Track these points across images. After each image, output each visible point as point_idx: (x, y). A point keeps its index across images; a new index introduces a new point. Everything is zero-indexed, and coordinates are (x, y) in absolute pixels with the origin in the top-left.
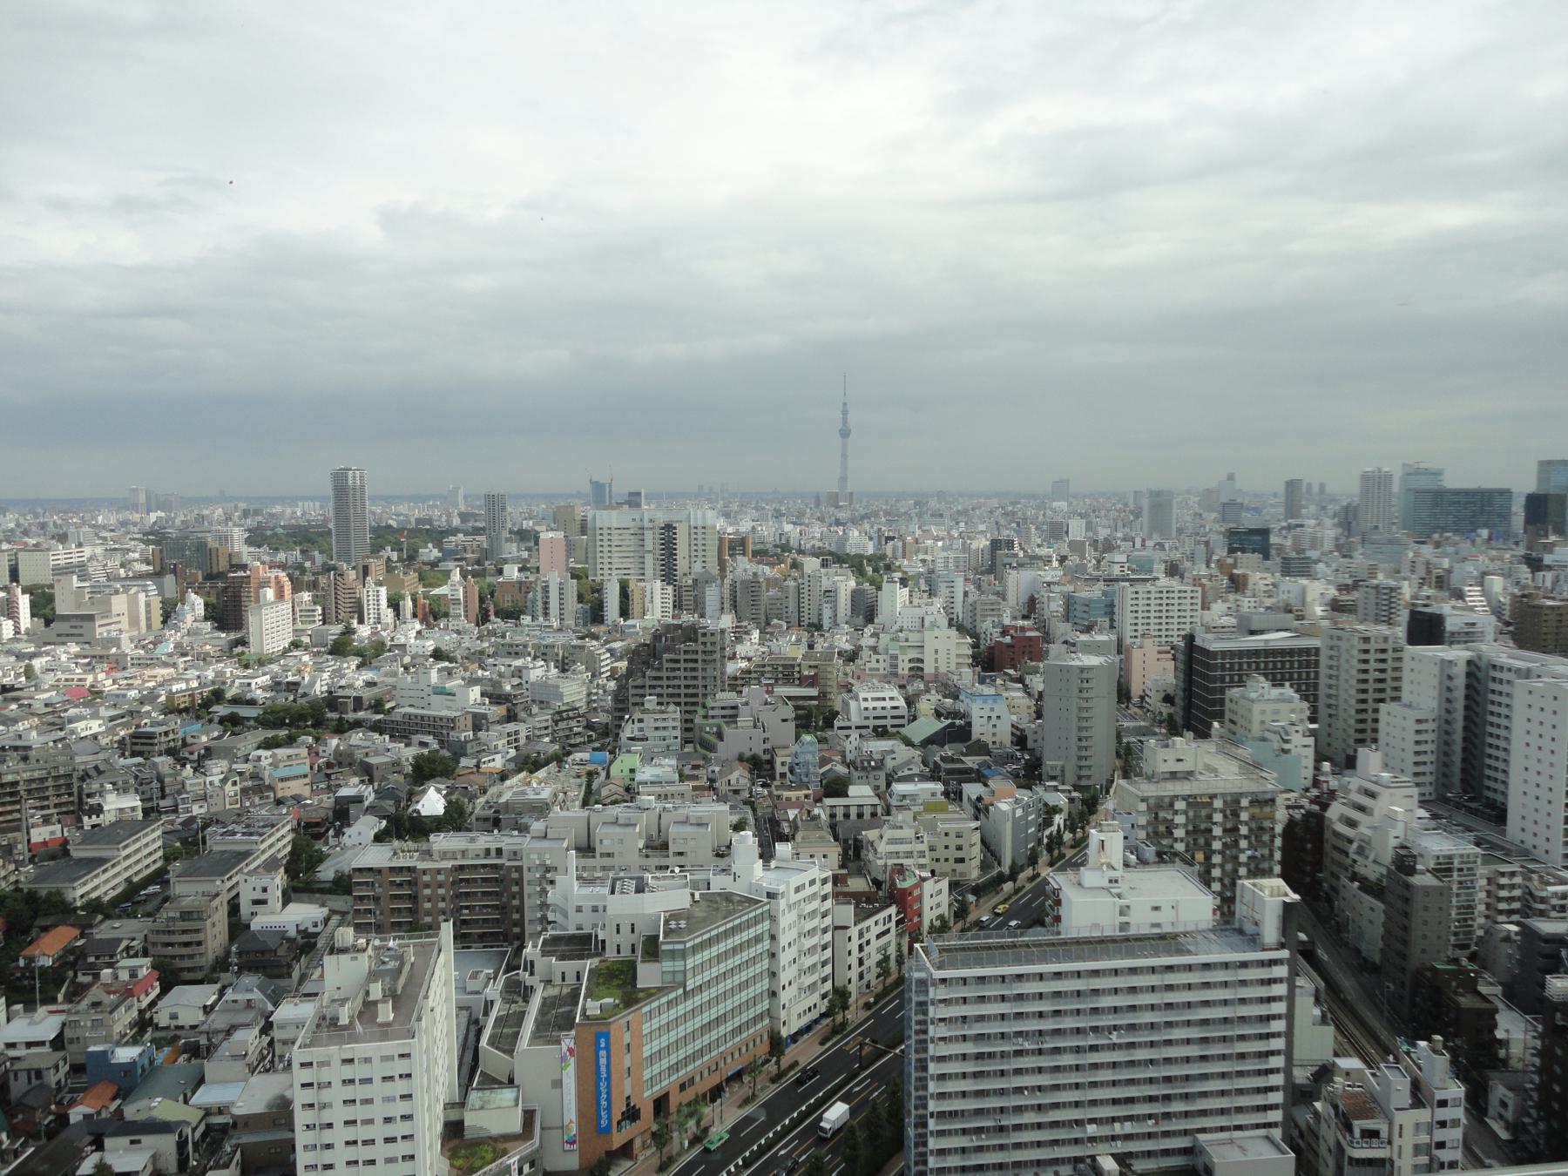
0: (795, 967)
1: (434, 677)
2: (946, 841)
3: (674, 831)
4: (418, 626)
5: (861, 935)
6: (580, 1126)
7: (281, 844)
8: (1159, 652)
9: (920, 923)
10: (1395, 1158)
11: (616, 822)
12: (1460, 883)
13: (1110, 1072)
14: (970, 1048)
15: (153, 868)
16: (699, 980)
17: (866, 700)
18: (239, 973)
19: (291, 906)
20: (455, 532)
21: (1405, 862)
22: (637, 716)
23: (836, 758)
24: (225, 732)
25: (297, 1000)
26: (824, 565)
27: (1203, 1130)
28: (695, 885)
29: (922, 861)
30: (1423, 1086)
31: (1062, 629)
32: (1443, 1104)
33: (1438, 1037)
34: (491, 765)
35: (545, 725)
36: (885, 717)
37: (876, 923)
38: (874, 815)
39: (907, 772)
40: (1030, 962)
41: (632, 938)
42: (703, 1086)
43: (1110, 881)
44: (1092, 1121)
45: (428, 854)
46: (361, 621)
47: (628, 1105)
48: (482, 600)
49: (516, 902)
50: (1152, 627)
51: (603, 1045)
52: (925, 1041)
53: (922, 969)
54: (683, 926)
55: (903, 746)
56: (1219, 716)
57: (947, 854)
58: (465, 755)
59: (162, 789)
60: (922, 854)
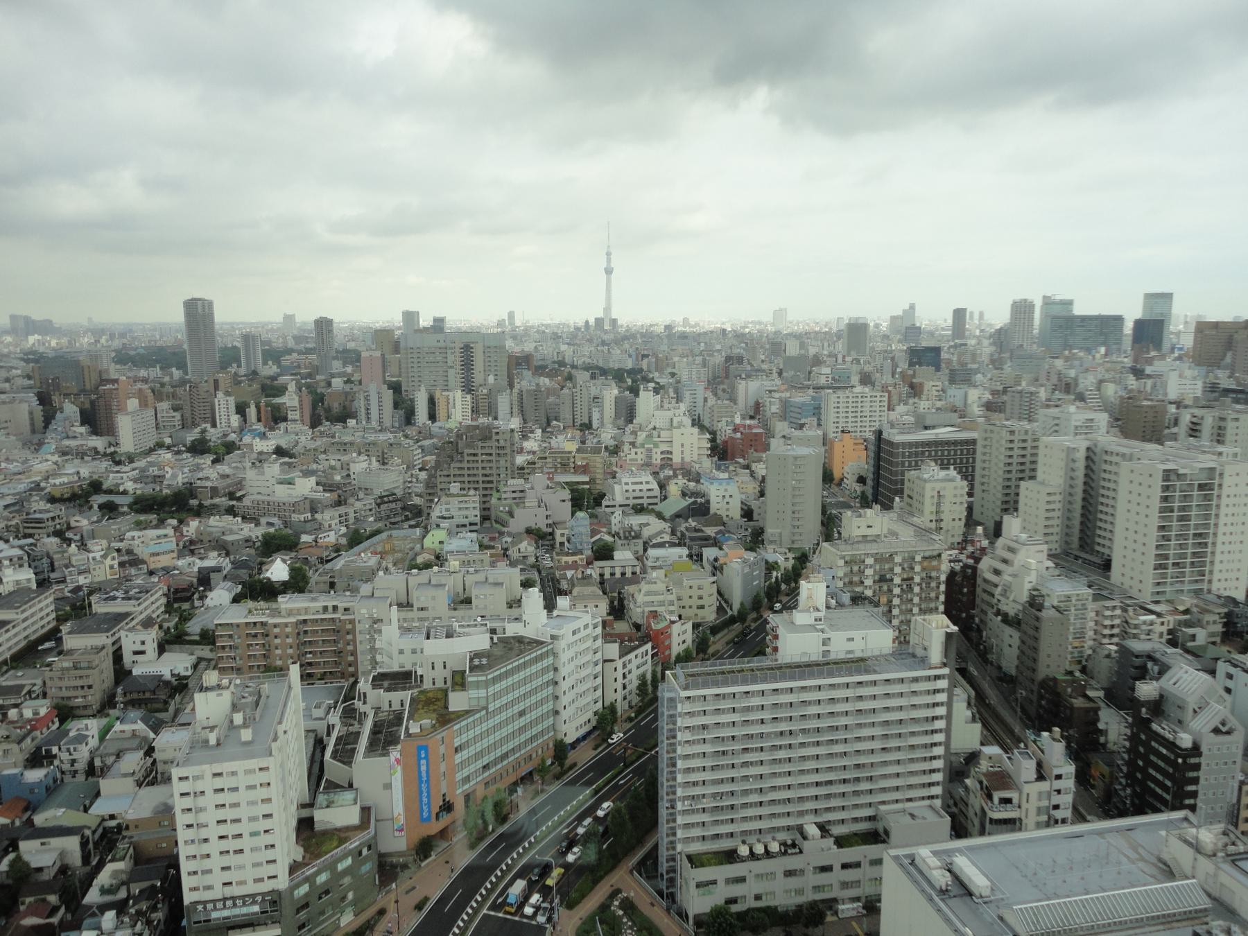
5: (624, 666)
6: (406, 819)
7: (154, 606)
8: (855, 444)
10: (1023, 818)
12: (1076, 615)
13: (813, 762)
14: (708, 748)
15: (51, 626)
16: (498, 704)
17: (627, 484)
18: (125, 708)
19: (165, 654)
20: (289, 351)
21: (1035, 603)
22: (444, 499)
24: (103, 516)
25: (173, 729)
26: (593, 377)
27: (883, 803)
29: (672, 608)
30: (1045, 765)
31: (781, 427)
32: (1059, 777)
33: (1057, 729)
34: (326, 540)
36: (642, 498)
37: (636, 657)
38: (634, 573)
39: (659, 540)
46: (214, 425)
47: (444, 800)
48: (314, 407)
49: (350, 648)
50: (850, 425)
51: (423, 756)
52: (674, 744)
53: (673, 690)
56: (900, 492)
57: (690, 602)
59: (52, 564)
60: (671, 603)
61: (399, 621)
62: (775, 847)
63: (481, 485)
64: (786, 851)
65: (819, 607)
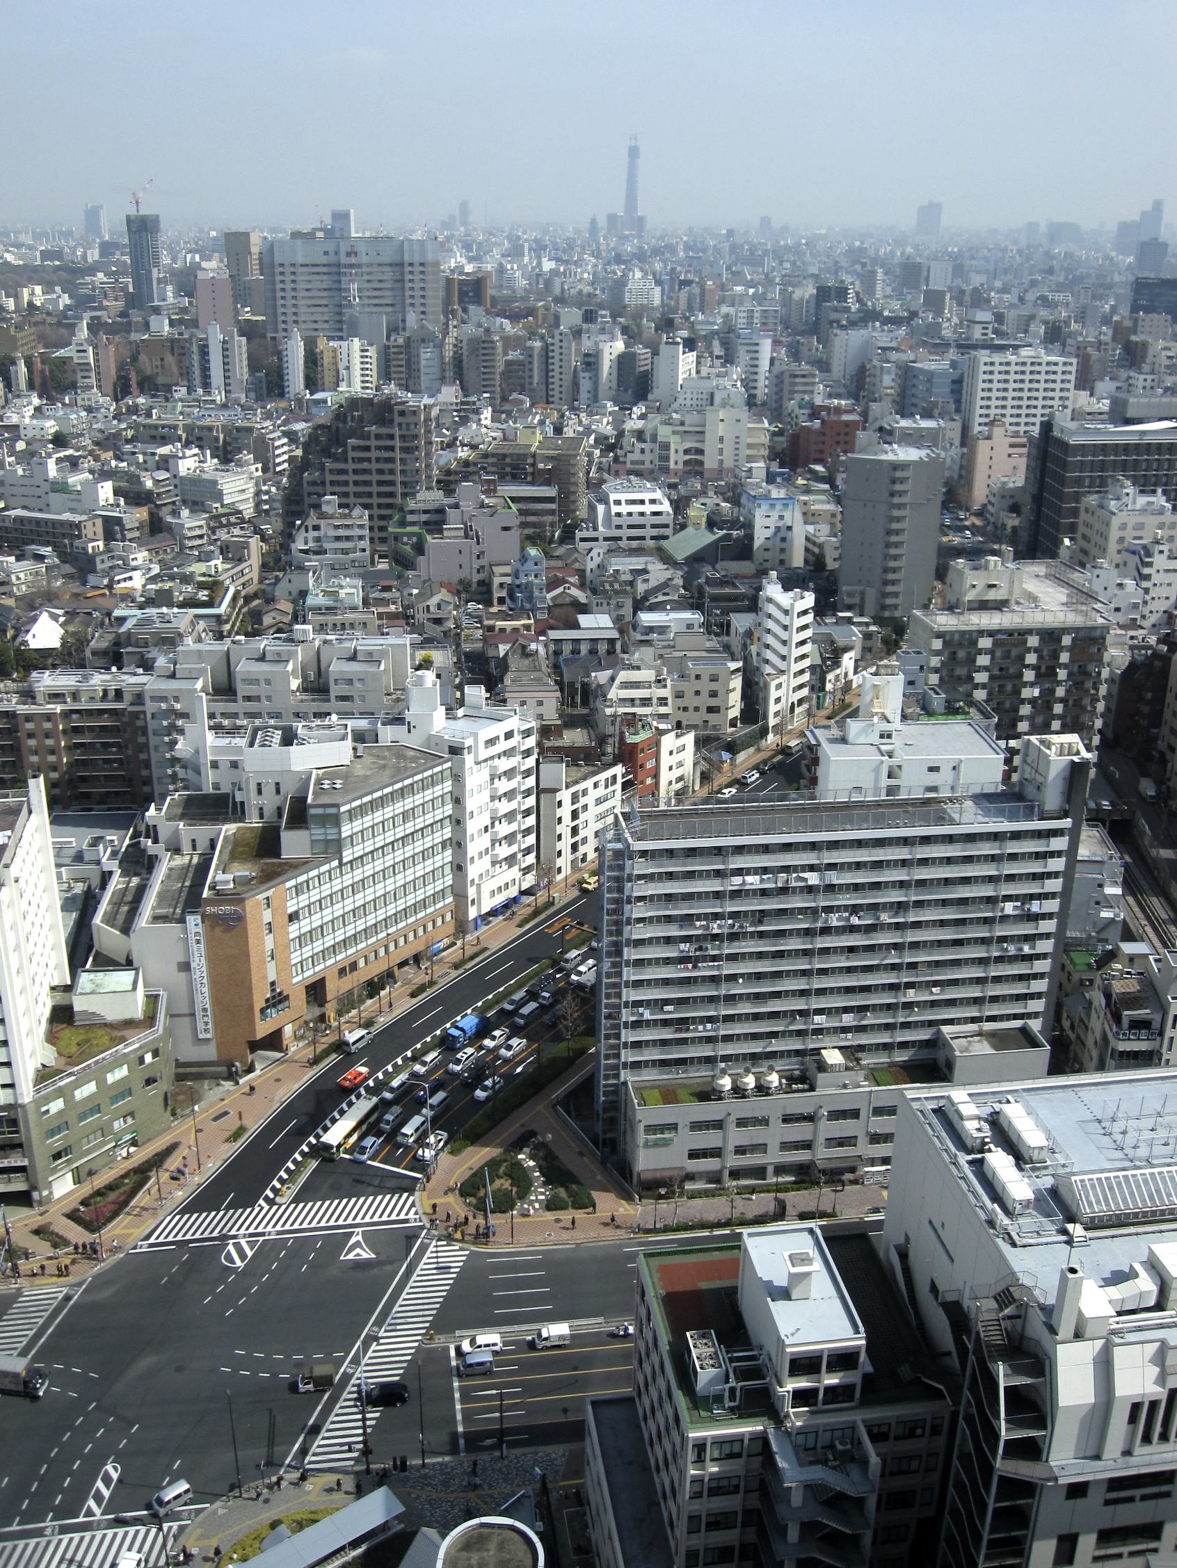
0: (487, 836)
1: (52, 470)
2: (697, 685)
3: (337, 668)
4: (36, 401)
8: (1012, 446)
9: (657, 784)
10: (1164, 1050)
11: (262, 658)
16: (358, 851)
17: (618, 503)
20: (92, 270)
22: (311, 521)
23: (571, 580)
27: (950, 1022)
28: (359, 737)
29: (663, 710)
31: (881, 411)
34: (128, 584)
35: (198, 532)
36: (642, 526)
37: (596, 785)
38: (611, 652)
39: (661, 598)
40: (753, 832)
41: (277, 800)
42: (366, 972)
43: (882, 736)
44: (819, 1012)
45: (28, 695)
47: (273, 990)
49: (143, 756)
54: (338, 786)
55: (661, 566)
56: (1072, 530)
57: (696, 701)
58: (94, 571)
60: (663, 701)
61: (211, 716)
62: (774, 1079)
63: (375, 501)
64: (790, 1085)
65: (890, 717)
